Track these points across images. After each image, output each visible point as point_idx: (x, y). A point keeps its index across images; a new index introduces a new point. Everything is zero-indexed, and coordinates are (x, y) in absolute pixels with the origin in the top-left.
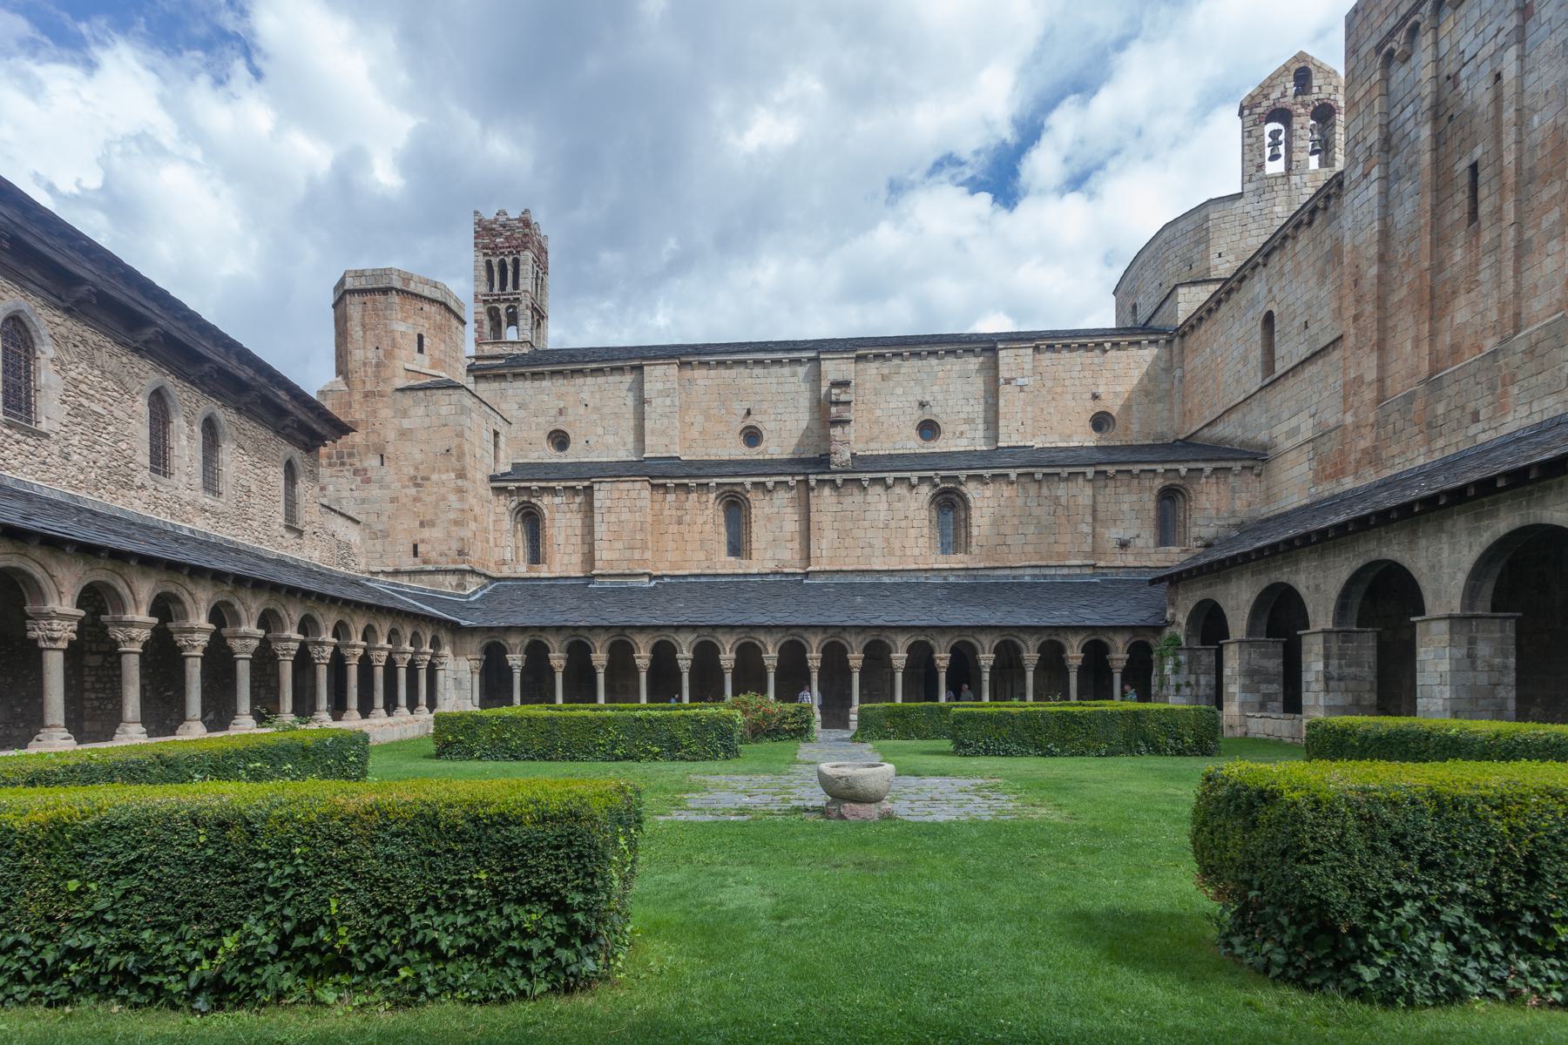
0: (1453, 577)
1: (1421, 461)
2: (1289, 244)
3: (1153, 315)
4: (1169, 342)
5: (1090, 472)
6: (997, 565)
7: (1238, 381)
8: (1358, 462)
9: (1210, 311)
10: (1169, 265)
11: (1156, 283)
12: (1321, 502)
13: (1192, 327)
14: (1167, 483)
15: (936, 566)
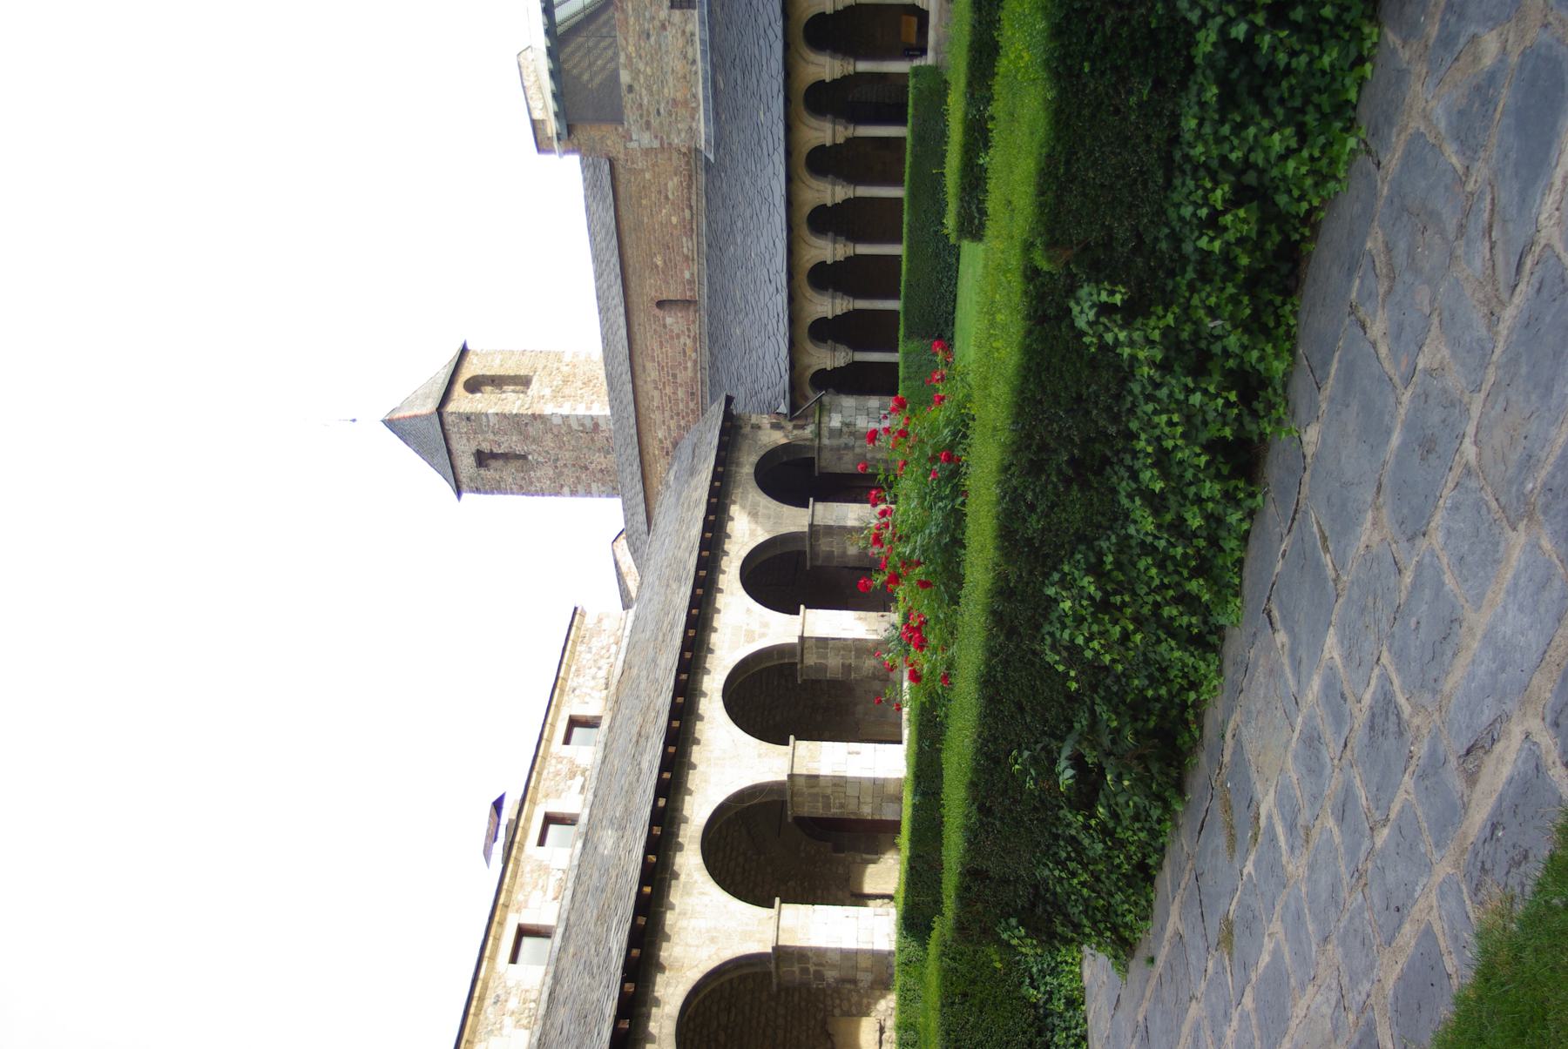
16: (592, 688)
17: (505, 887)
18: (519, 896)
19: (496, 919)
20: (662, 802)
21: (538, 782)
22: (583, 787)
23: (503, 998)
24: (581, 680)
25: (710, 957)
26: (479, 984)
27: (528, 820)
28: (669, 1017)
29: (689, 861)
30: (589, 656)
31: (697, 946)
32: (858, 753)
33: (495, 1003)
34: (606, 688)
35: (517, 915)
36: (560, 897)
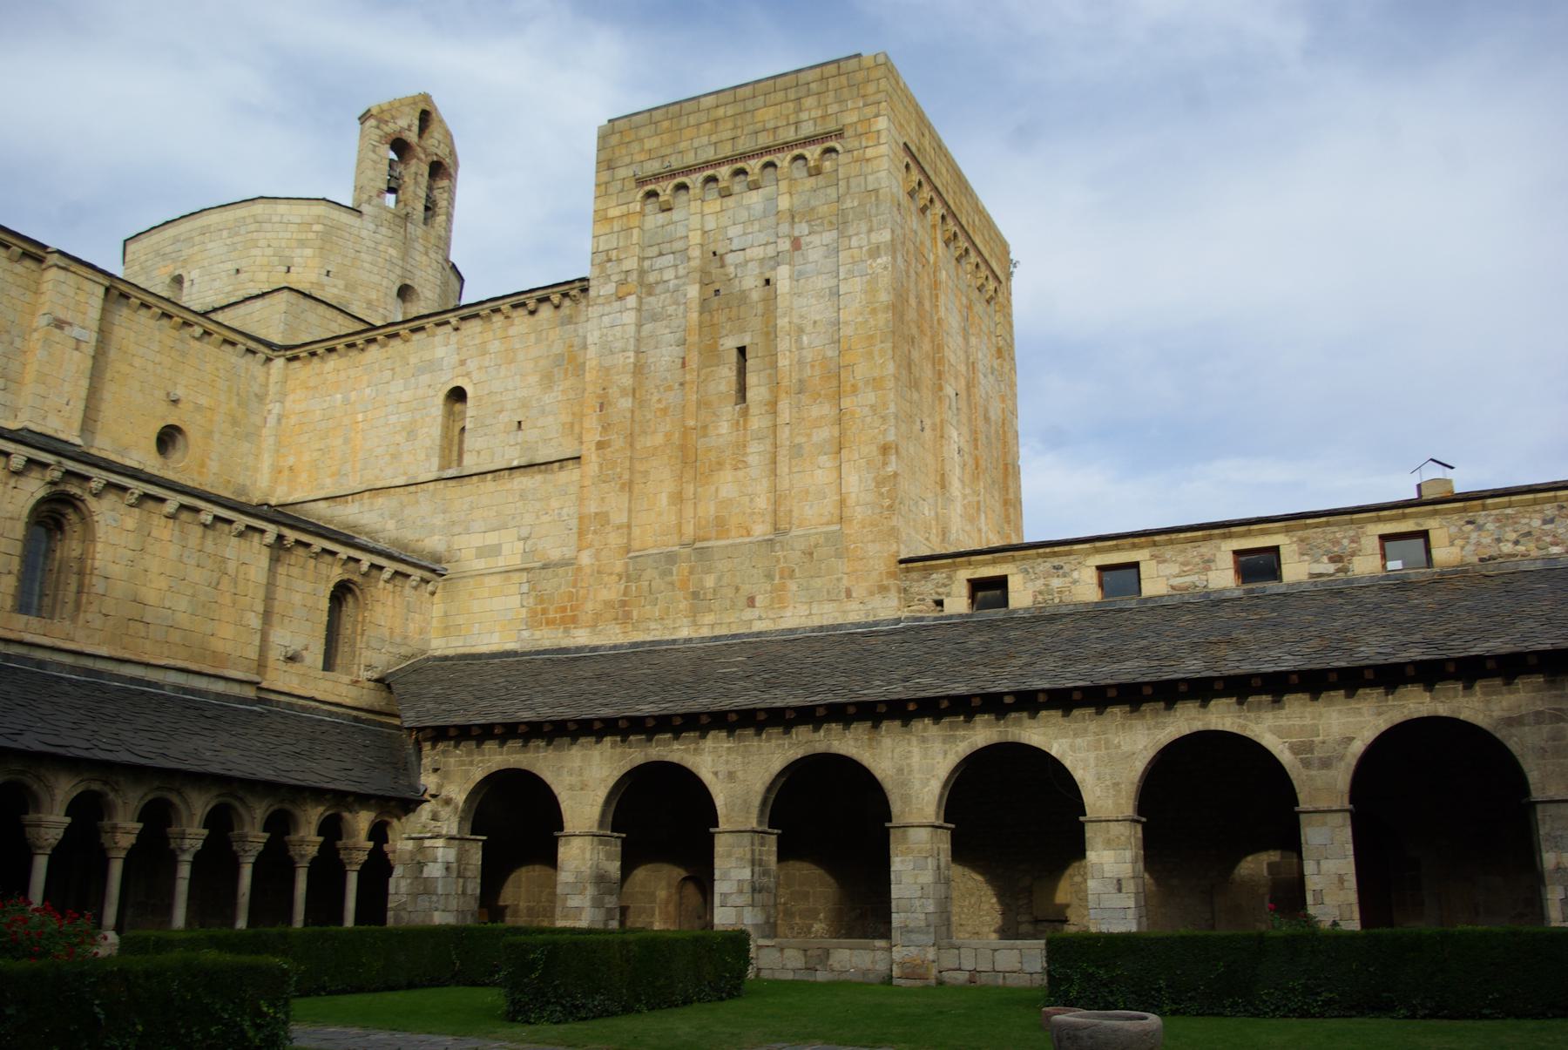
0: (925, 783)
1: (684, 633)
2: (497, 318)
3: (222, 308)
4: (269, 360)
5: (272, 530)
6: (127, 656)
7: (394, 457)
8: (598, 616)
9: (351, 346)
10: (254, 252)
11: (231, 266)
12: (538, 653)
13: (313, 354)
14: (346, 577)
15: (28, 637)
16: (1478, 544)
17: (1174, 536)
18: (1168, 552)
19: (1136, 540)
20: (1008, 700)
21: (1317, 526)
22: (1320, 575)
23: (1061, 571)
24: (1490, 526)
25: (883, 770)
26: (1067, 548)
27: (1264, 533)
28: (829, 746)
29: (982, 734)
30: (1536, 523)
31: (892, 758)
32: (1120, 890)
33: (1054, 567)
34: (1482, 560)
35: (1148, 557)
36: (1174, 592)
